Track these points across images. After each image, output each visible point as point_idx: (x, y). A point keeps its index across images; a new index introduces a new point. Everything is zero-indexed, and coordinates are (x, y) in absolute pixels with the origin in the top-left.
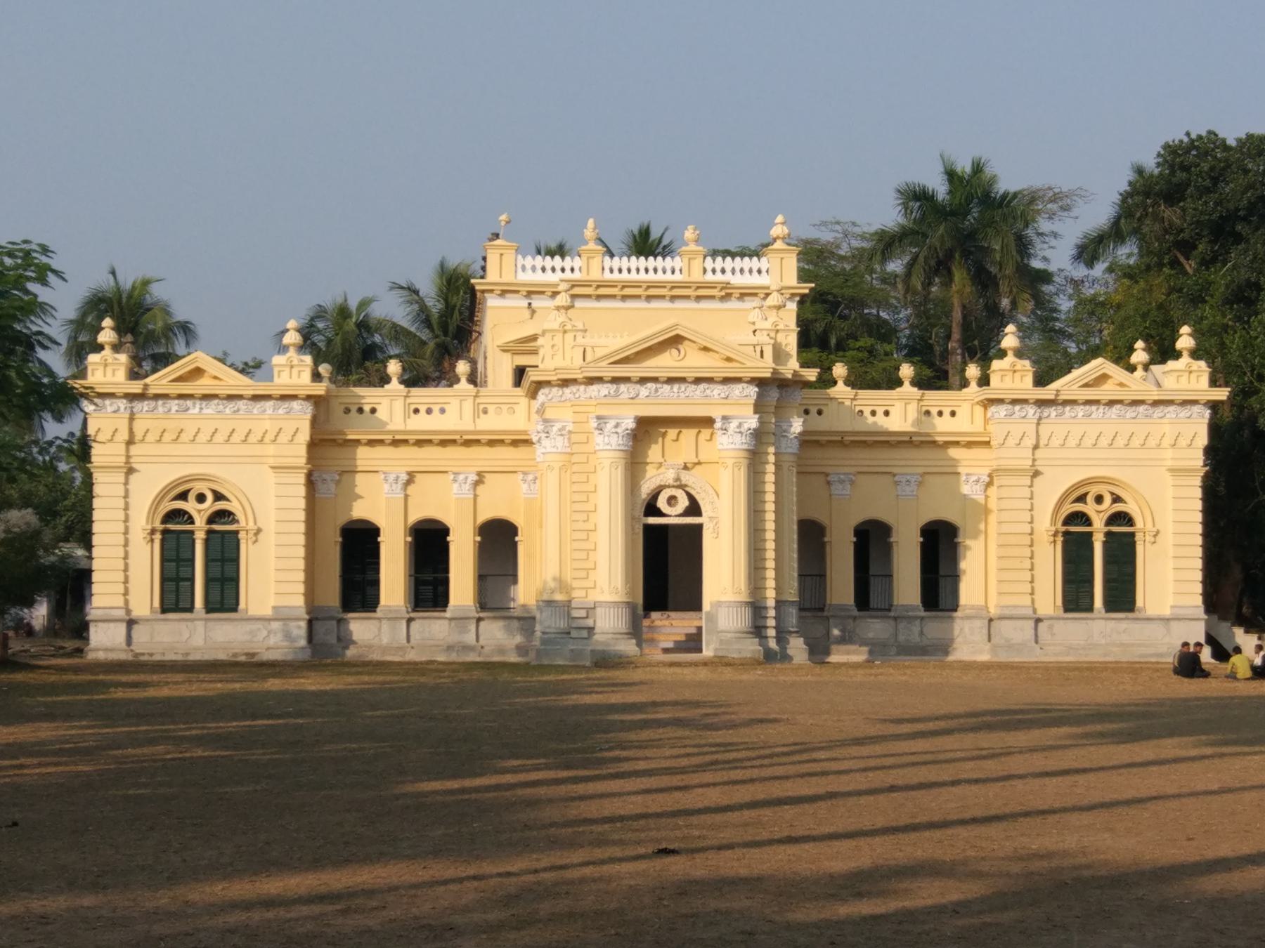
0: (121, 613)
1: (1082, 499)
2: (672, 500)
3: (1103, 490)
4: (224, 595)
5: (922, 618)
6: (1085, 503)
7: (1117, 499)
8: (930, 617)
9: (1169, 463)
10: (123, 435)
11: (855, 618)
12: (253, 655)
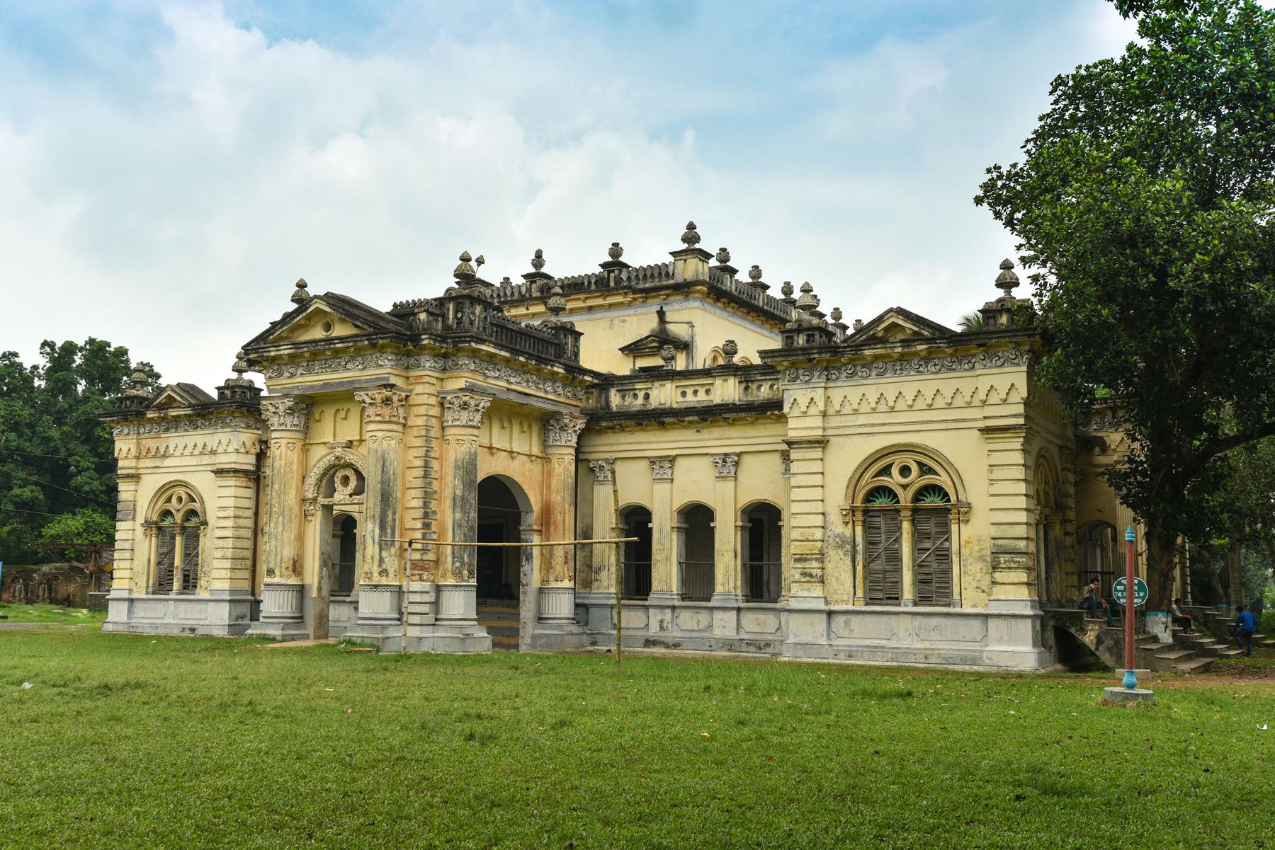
0: (125, 595)
1: (886, 471)
2: (346, 480)
3: (909, 460)
4: (190, 583)
5: (739, 610)
6: (890, 475)
7: (925, 470)
8: (749, 609)
9: (982, 424)
10: (134, 450)
11: (673, 608)
12: (193, 630)
